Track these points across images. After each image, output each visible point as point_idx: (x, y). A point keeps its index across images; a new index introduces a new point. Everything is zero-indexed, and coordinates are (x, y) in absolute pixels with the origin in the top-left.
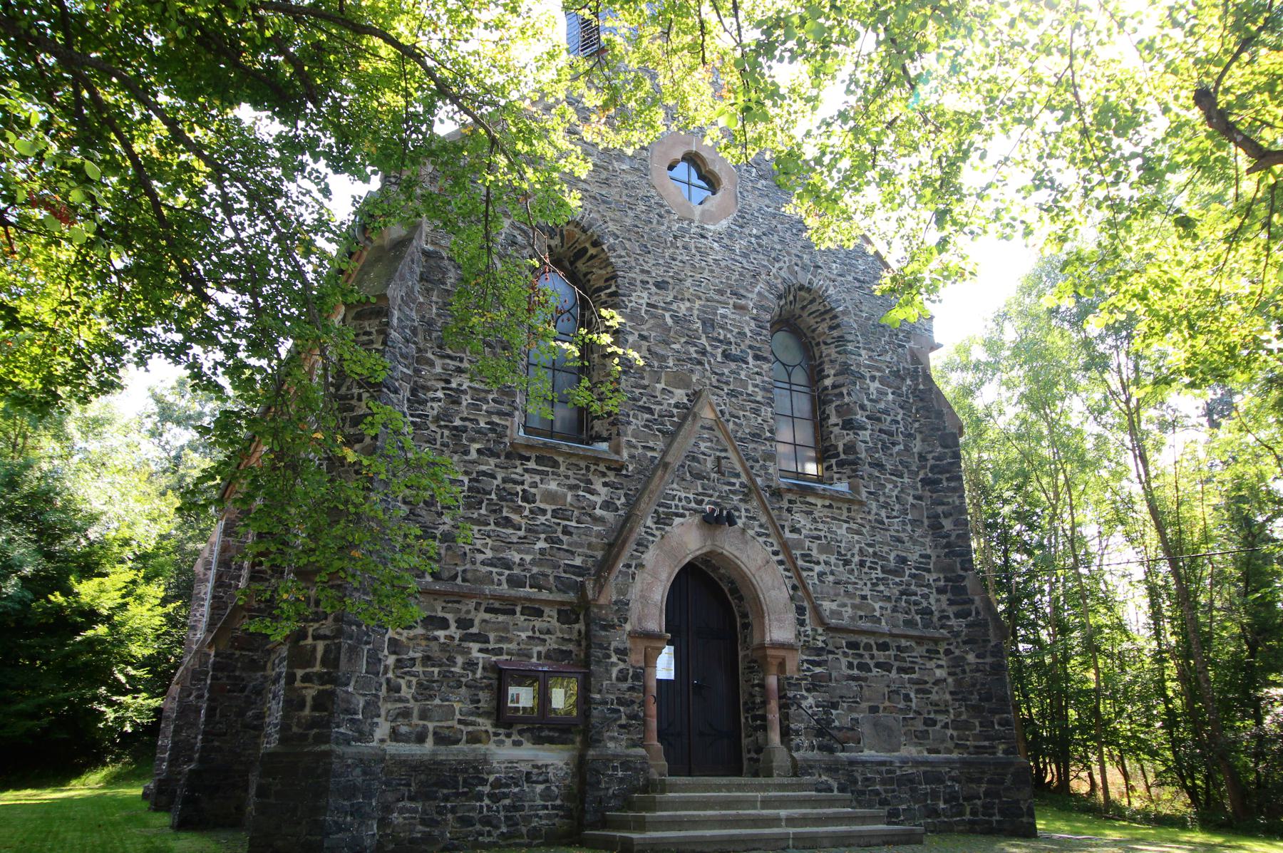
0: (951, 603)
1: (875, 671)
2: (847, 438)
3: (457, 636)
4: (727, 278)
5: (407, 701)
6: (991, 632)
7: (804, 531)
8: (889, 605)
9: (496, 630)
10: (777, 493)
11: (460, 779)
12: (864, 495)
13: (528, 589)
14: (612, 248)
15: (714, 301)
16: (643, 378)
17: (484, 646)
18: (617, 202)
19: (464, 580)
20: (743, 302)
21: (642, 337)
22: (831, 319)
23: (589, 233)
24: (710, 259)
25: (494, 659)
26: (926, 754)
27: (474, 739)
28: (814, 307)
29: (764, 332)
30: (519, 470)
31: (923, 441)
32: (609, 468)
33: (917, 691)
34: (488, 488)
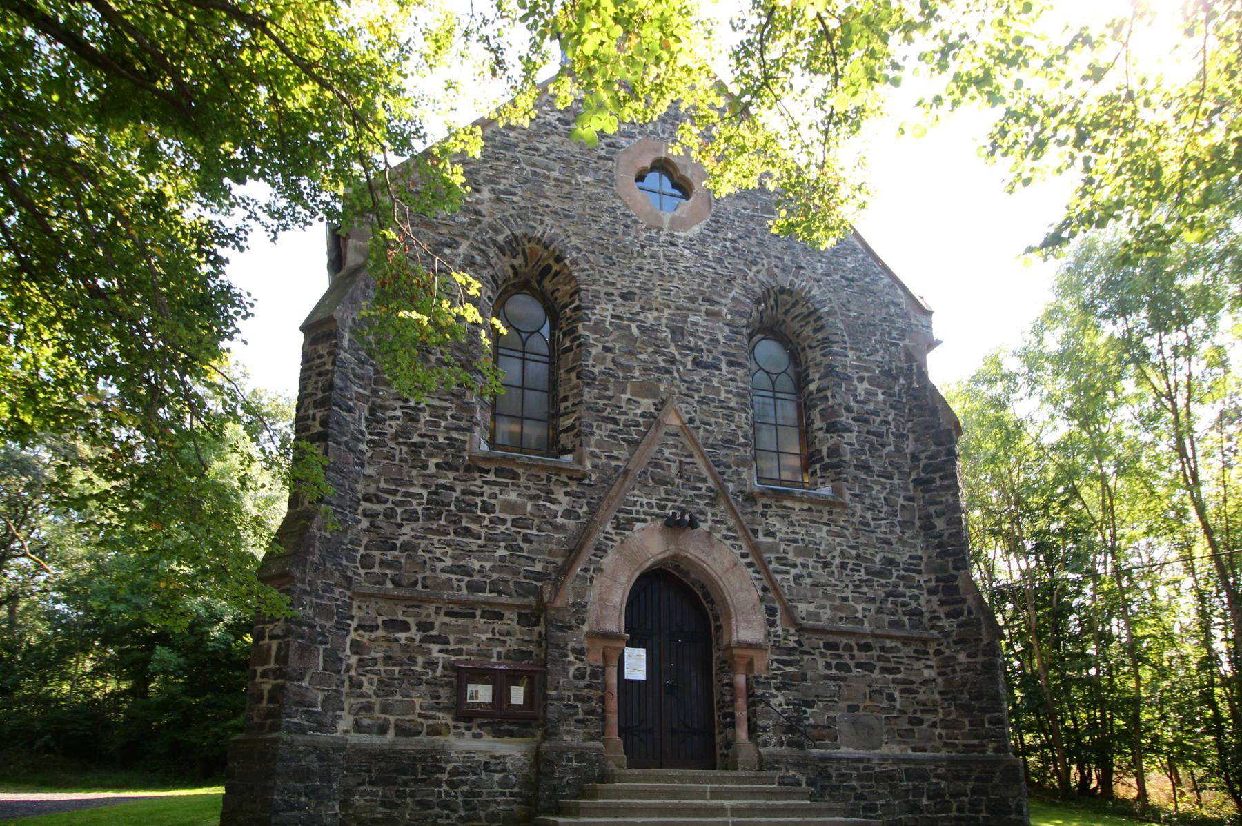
0: (942, 603)
1: (855, 671)
2: (831, 442)
3: (418, 638)
4: (699, 285)
5: (369, 696)
6: (984, 630)
7: (779, 535)
8: (873, 607)
9: (456, 632)
10: (751, 498)
11: (419, 767)
12: (847, 497)
13: (488, 594)
14: (575, 262)
15: (683, 308)
16: (607, 389)
17: (444, 647)
18: (580, 216)
19: (424, 586)
20: (716, 308)
21: (606, 349)
23: (551, 249)
25: (454, 658)
26: (910, 752)
27: (434, 731)
29: (739, 337)
30: (478, 482)
31: (916, 440)
32: (570, 478)
33: (902, 691)
34: (447, 501)
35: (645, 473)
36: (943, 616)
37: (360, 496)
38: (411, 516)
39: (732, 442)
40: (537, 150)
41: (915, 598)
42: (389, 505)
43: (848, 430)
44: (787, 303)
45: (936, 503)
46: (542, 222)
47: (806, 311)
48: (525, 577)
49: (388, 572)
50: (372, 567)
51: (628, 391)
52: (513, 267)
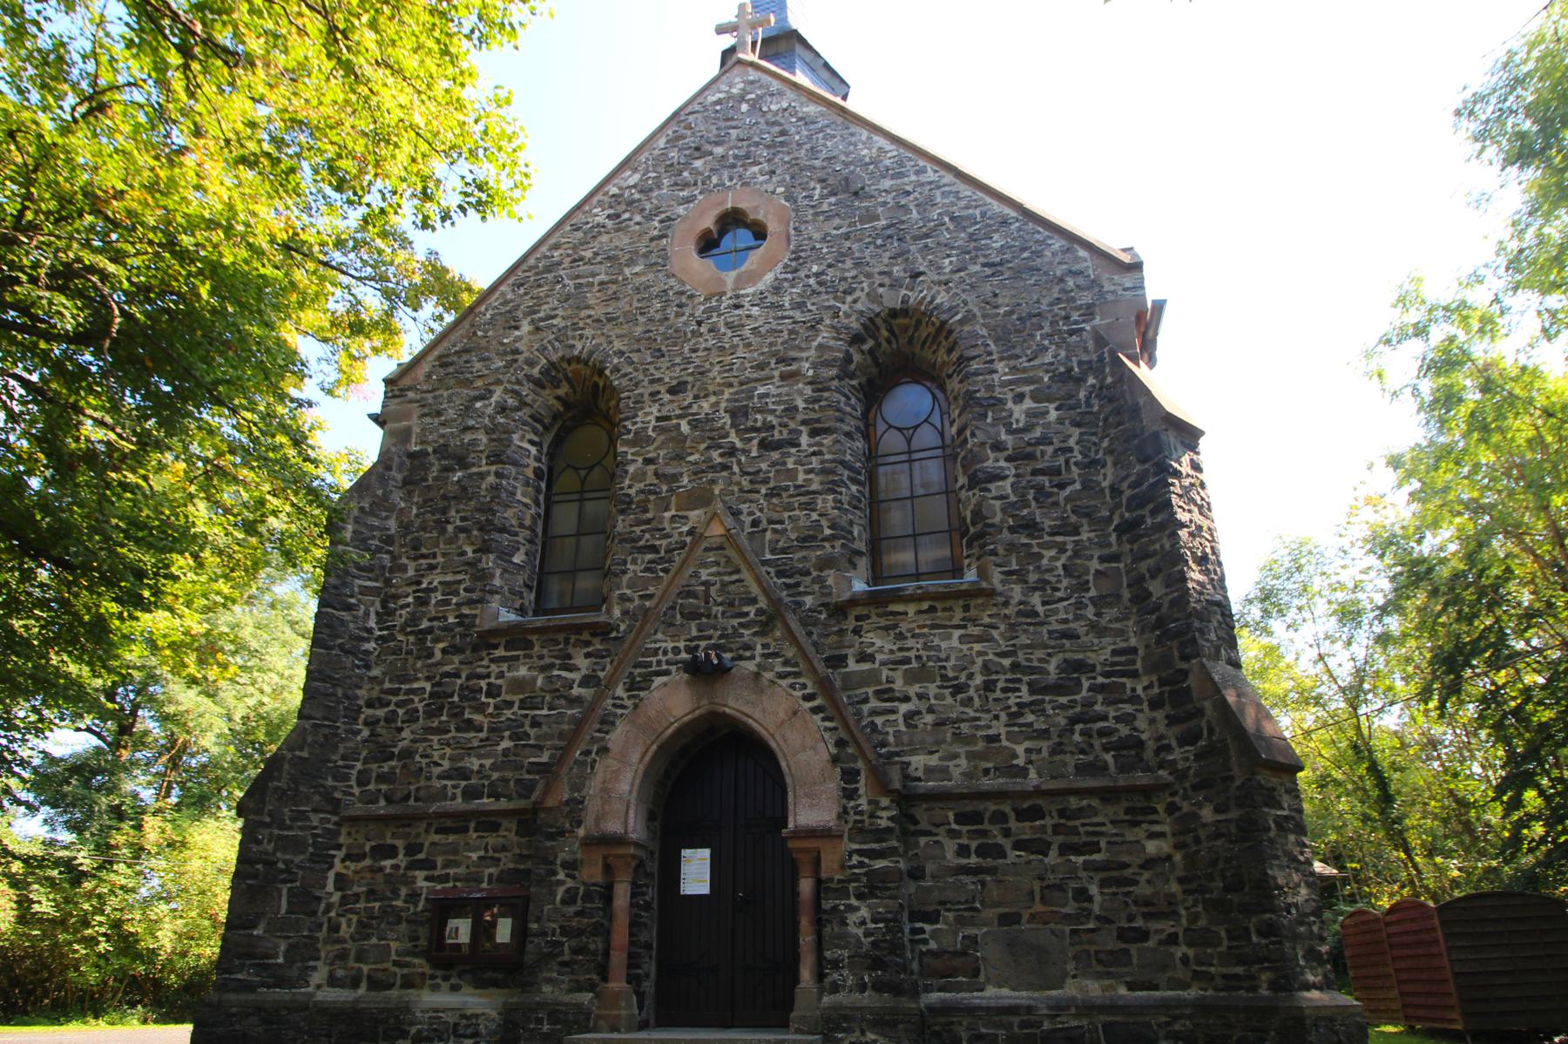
1: (1012, 855)
2: (973, 501)
3: (403, 865)
4: (771, 345)
5: (345, 941)
7: (879, 657)
8: (1045, 745)
9: (444, 853)
10: (839, 610)
11: (380, 1030)
12: (996, 577)
14: (616, 369)
15: (750, 381)
16: (646, 511)
18: (625, 314)
19: (417, 800)
20: (794, 367)
21: (648, 461)
22: (947, 338)
24: (746, 332)
25: (439, 887)
26: (1123, 991)
27: (408, 983)
28: (924, 332)
29: (826, 394)
31: (1115, 464)
32: (593, 635)
33: (1103, 884)
34: (449, 690)
35: (673, 608)
36: (1174, 744)
38: (412, 717)
39: (813, 538)
40: (581, 259)
41: (1128, 719)
42: (392, 707)
43: (999, 477)
44: (907, 327)
45: (1147, 556)
46: (581, 337)
47: (931, 329)
48: (529, 772)
49: (384, 787)
50: (368, 783)
51: (673, 506)
52: (558, 398)
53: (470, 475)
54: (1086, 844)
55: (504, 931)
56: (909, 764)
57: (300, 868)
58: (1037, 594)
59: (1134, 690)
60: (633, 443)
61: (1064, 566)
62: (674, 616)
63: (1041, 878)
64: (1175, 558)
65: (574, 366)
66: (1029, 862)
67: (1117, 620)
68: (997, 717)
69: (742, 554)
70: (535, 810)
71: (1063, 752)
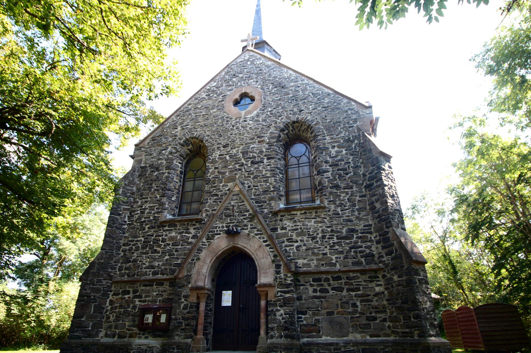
1: (331, 292)
2: (319, 179)
3: (132, 297)
4: (255, 132)
5: (111, 322)
7: (288, 228)
8: (342, 256)
9: (145, 293)
10: (275, 214)
12: (326, 203)
15: (248, 143)
16: (215, 183)
18: (210, 124)
21: (216, 168)
24: (248, 129)
25: (143, 304)
26: (368, 337)
27: (131, 336)
28: (303, 128)
29: (272, 147)
31: (364, 167)
32: (196, 222)
33: (361, 301)
34: (149, 240)
35: (222, 214)
36: (384, 255)
37: (121, 244)
38: (137, 249)
39: (267, 191)
41: (369, 247)
42: (131, 246)
44: (298, 127)
45: (375, 195)
46: (196, 131)
47: (306, 127)
49: (127, 271)
50: (122, 270)
51: (223, 182)
52: (188, 149)
53: (160, 173)
54: (355, 288)
55: (163, 319)
56: (297, 262)
57: (98, 298)
58: (339, 208)
59: (371, 238)
60: (211, 163)
61: (348, 199)
62: (222, 216)
63: (341, 300)
64: (384, 196)
65: (194, 140)
66: (337, 294)
67: (365, 216)
68: (326, 247)
69: (244, 196)
70: (175, 278)
71: (348, 258)
